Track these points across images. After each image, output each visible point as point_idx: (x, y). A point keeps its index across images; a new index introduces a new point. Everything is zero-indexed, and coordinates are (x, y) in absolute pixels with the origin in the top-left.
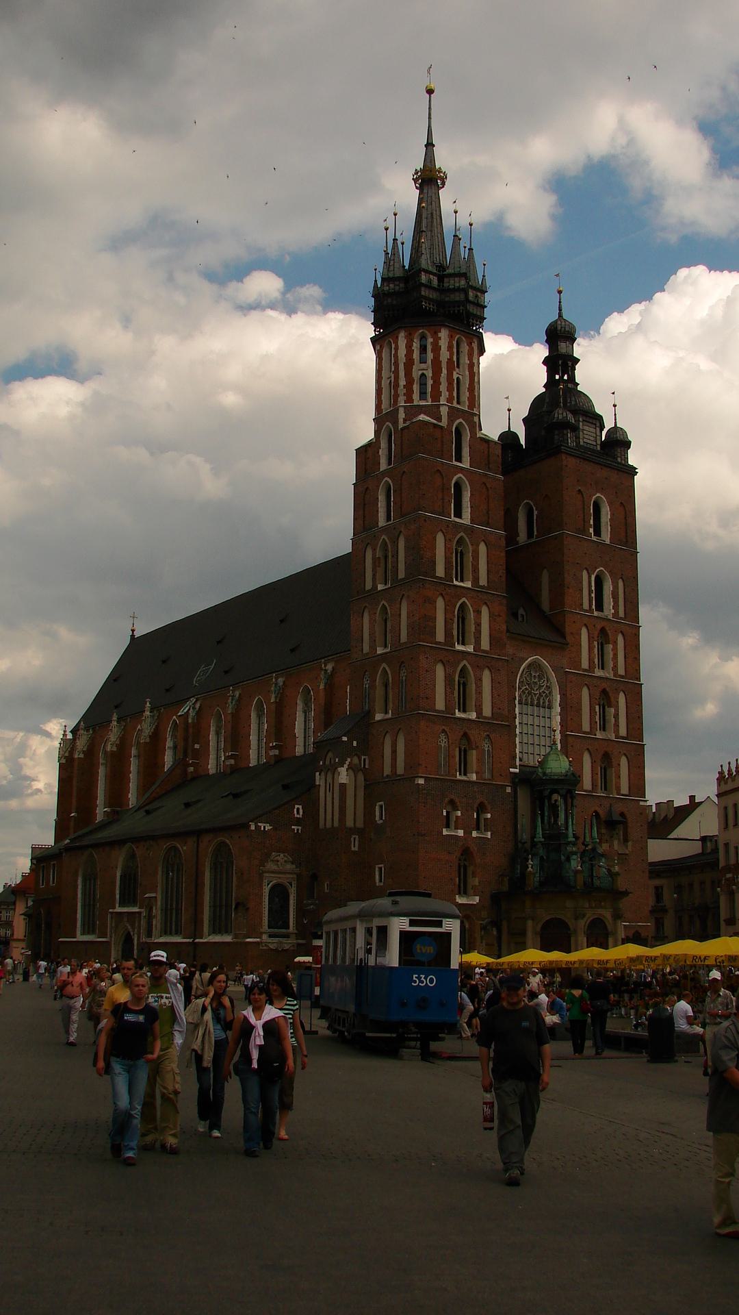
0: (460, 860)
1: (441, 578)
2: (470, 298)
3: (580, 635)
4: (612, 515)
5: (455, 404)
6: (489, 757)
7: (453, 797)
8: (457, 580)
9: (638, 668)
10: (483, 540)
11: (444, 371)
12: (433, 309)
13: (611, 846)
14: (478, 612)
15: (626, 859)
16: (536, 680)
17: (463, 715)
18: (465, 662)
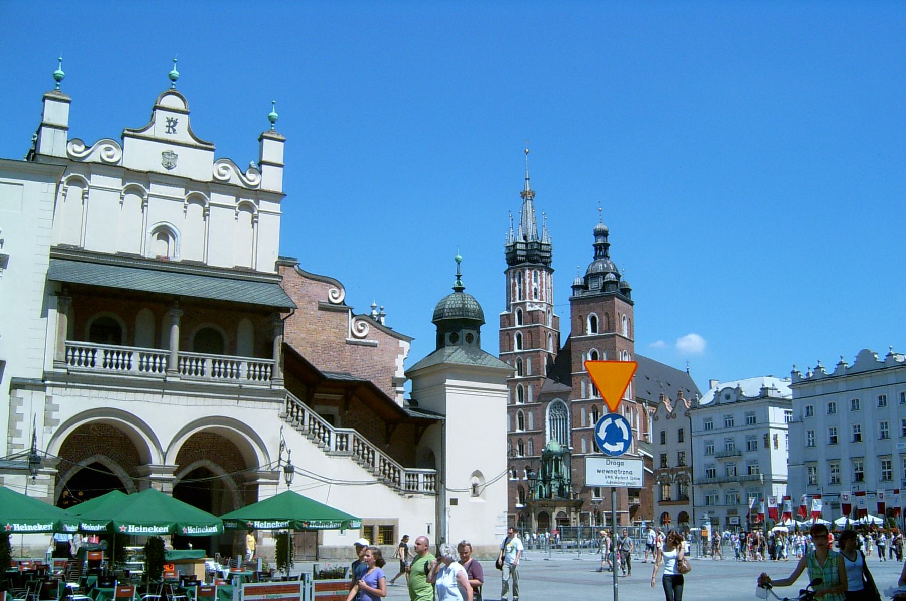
2: (529, 249)
5: (518, 301)
7: (513, 465)
14: (527, 387)
18: (520, 409)
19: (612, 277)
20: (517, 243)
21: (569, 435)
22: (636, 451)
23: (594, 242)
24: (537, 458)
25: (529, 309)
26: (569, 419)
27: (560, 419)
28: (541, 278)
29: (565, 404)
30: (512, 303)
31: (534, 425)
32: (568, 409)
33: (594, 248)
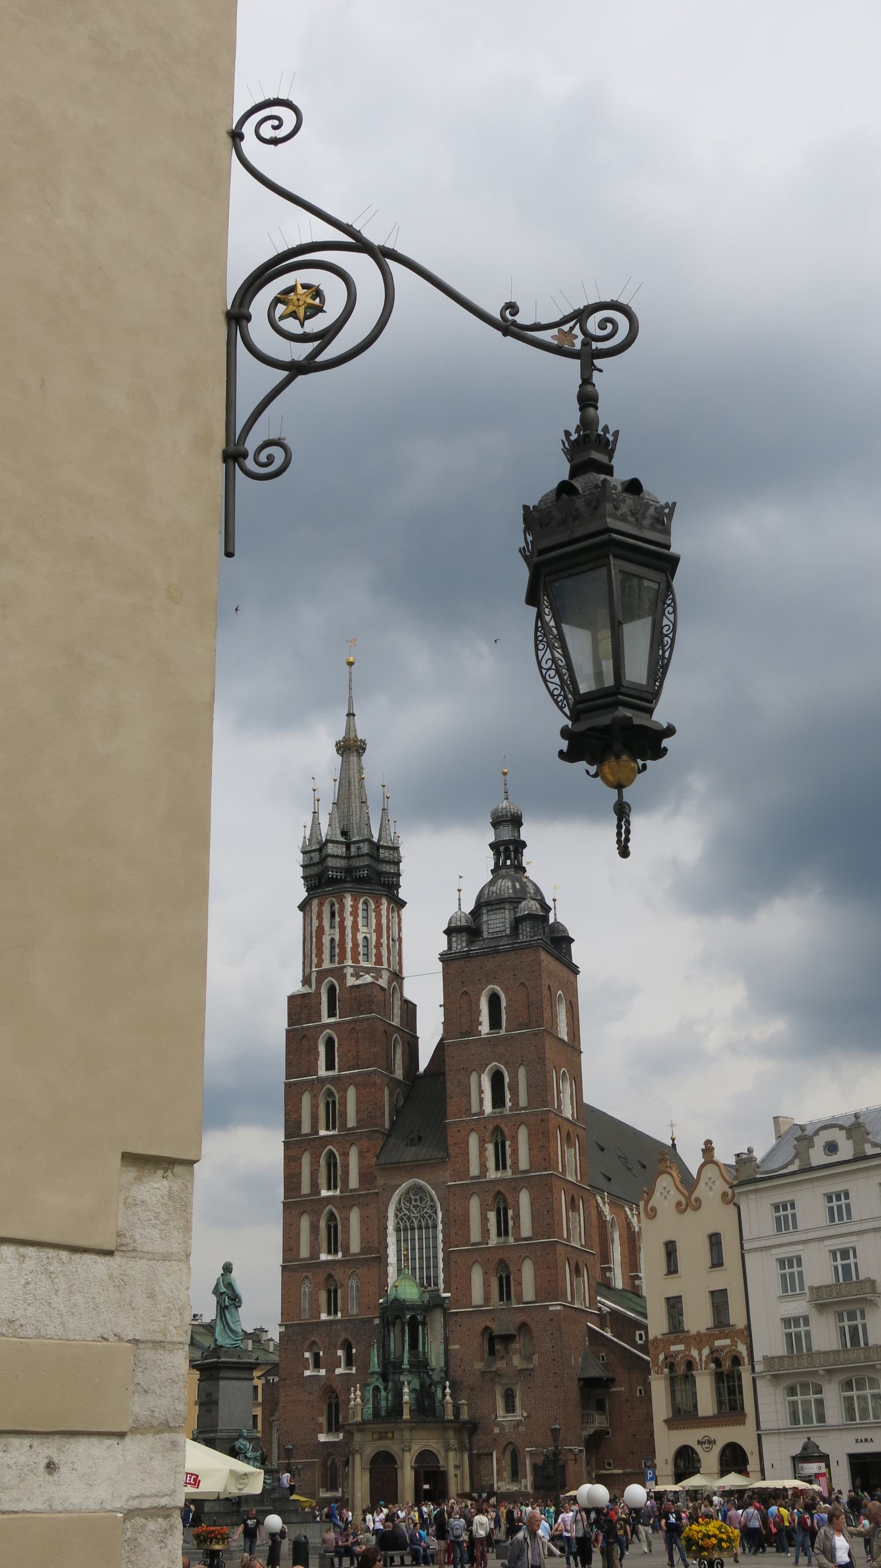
0: (330, 1397)
1: (305, 1135)
2: (353, 854)
3: (467, 1143)
4: (509, 1000)
5: (326, 965)
6: (358, 1291)
7: (314, 1338)
8: (328, 1129)
9: (545, 1157)
10: (351, 1084)
11: (314, 940)
12: (315, 884)
13: (510, 1362)
14: (346, 1155)
15: (530, 1374)
16: (418, 1203)
17: (330, 1258)
18: (330, 1207)
19: (533, 906)
20: (327, 841)
21: (441, 1265)
22: (593, 1302)
23: (492, 839)
24: (370, 1320)
25: (351, 981)
26: (440, 1227)
27: (420, 1228)
28: (379, 916)
29: (433, 1192)
30: (314, 969)
31: (361, 1243)
32: (438, 1205)
33: (490, 853)
